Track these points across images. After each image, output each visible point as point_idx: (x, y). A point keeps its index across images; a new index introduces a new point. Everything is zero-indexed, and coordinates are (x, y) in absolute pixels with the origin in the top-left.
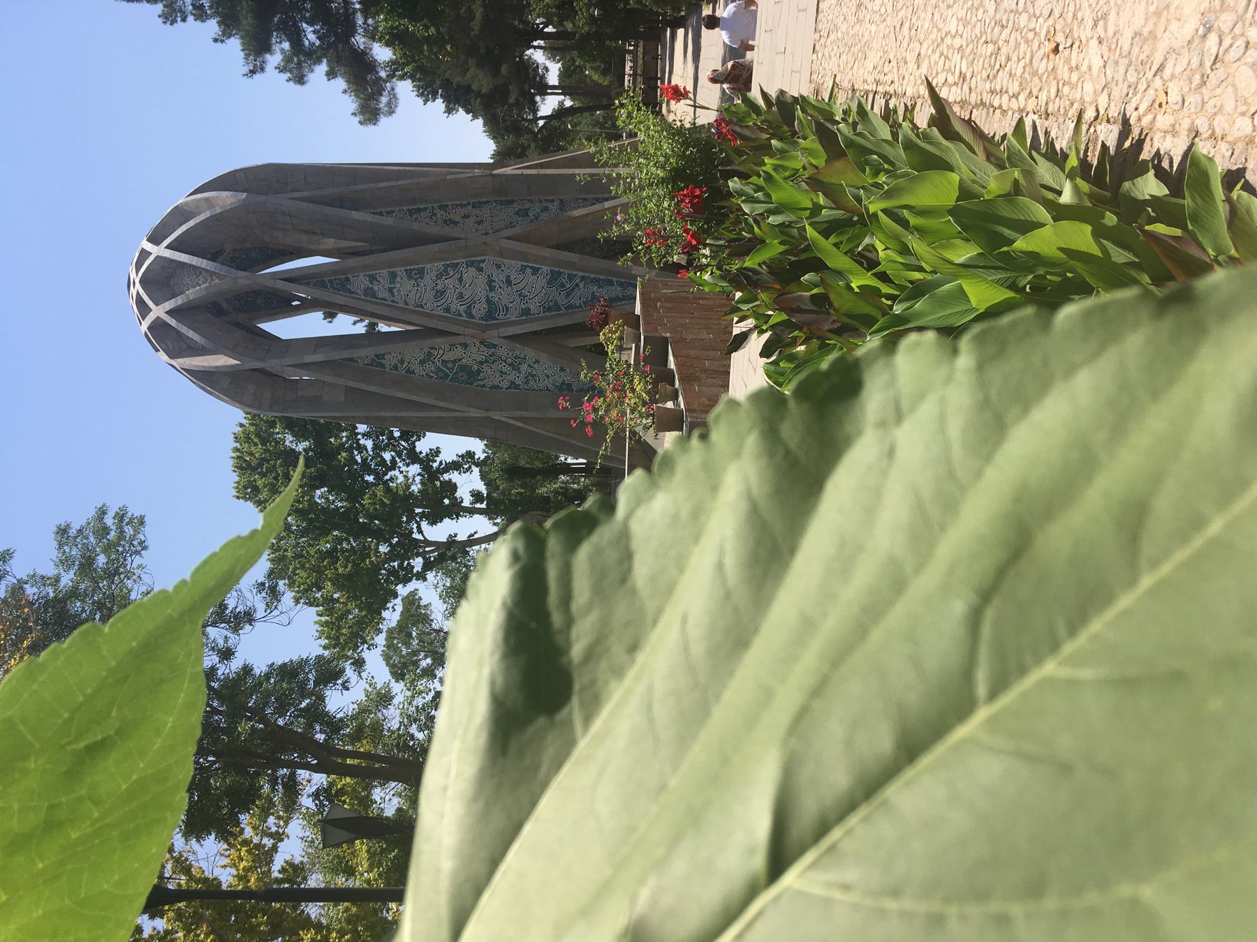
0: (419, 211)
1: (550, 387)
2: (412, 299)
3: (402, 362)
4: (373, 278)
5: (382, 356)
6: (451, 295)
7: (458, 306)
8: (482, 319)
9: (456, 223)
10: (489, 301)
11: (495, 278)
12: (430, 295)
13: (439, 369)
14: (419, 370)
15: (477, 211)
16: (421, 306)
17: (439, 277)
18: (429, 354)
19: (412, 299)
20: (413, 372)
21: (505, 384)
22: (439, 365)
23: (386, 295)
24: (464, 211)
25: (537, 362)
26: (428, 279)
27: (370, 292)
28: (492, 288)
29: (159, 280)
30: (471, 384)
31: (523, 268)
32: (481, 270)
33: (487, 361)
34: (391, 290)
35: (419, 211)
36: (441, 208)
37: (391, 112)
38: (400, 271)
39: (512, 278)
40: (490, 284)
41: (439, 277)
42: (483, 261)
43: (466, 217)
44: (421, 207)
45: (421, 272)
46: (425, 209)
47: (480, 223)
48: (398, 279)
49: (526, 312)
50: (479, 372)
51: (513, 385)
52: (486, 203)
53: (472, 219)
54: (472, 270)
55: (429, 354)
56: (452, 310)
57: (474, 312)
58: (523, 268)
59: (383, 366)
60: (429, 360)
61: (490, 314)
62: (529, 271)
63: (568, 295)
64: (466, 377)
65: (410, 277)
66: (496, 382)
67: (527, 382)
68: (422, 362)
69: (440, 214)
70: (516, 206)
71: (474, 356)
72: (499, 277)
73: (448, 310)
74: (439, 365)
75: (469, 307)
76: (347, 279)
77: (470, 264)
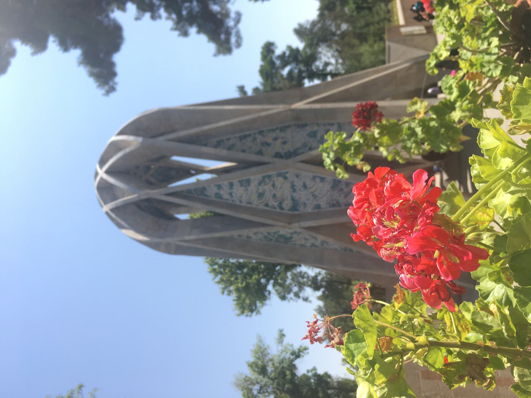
0: (246, 137)
2: (244, 199)
6: (268, 196)
7: (273, 203)
8: (289, 210)
9: (268, 144)
10: (293, 199)
11: (296, 183)
12: (254, 197)
15: (282, 134)
16: (250, 203)
17: (260, 184)
19: (244, 199)
20: (251, 238)
21: (308, 244)
24: (274, 135)
26: (253, 186)
27: (218, 196)
28: (294, 191)
29: (105, 191)
31: (314, 178)
32: (286, 178)
34: (231, 194)
35: (246, 137)
36: (261, 133)
37: (239, 45)
38: (235, 182)
39: (307, 184)
40: (293, 187)
43: (275, 139)
44: (247, 133)
45: (248, 182)
46: (250, 135)
48: (235, 187)
49: (318, 207)
50: (291, 238)
51: (313, 245)
52: (289, 127)
54: (281, 179)
56: (270, 203)
57: (284, 205)
58: (314, 178)
61: (294, 207)
62: (318, 180)
63: (346, 196)
65: (242, 185)
66: (303, 242)
69: (259, 138)
70: (308, 129)
72: (298, 183)
73: (267, 205)
75: (280, 203)
77: (279, 175)
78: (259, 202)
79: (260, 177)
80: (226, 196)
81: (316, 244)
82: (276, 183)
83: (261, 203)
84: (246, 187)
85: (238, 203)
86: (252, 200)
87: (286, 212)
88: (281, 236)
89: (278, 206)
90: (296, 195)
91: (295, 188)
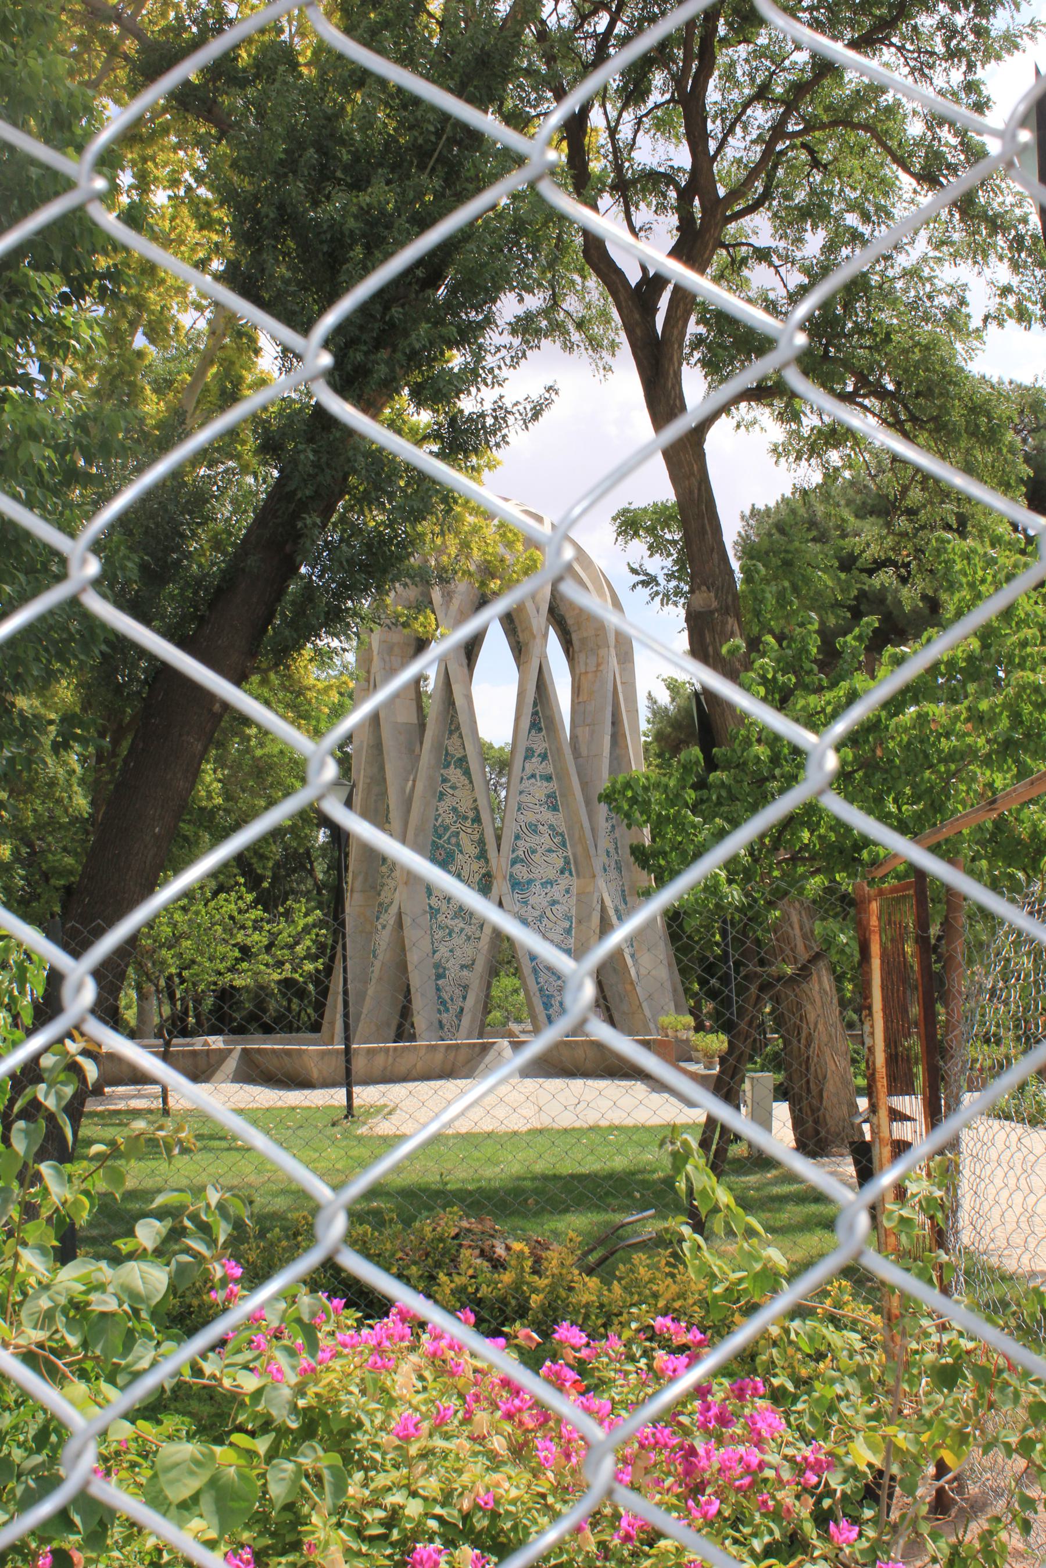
1: (437, 955)
3: (454, 788)
4: (544, 757)
6: (533, 840)
10: (530, 882)
12: (531, 817)
13: (446, 828)
14: (444, 806)
17: (551, 827)
18: (466, 818)
20: (440, 799)
23: (529, 771)
25: (469, 938)
26: (548, 816)
34: (533, 776)
38: (554, 785)
40: (551, 883)
41: (551, 827)
45: (555, 808)
54: (560, 863)
55: (466, 818)
57: (518, 866)
58: (569, 918)
62: (567, 924)
65: (548, 796)
67: (440, 927)
68: (455, 810)
71: (466, 867)
72: (556, 892)
76: (540, 730)
77: (567, 862)
79: (563, 829)
81: (441, 917)
90: (536, 888)
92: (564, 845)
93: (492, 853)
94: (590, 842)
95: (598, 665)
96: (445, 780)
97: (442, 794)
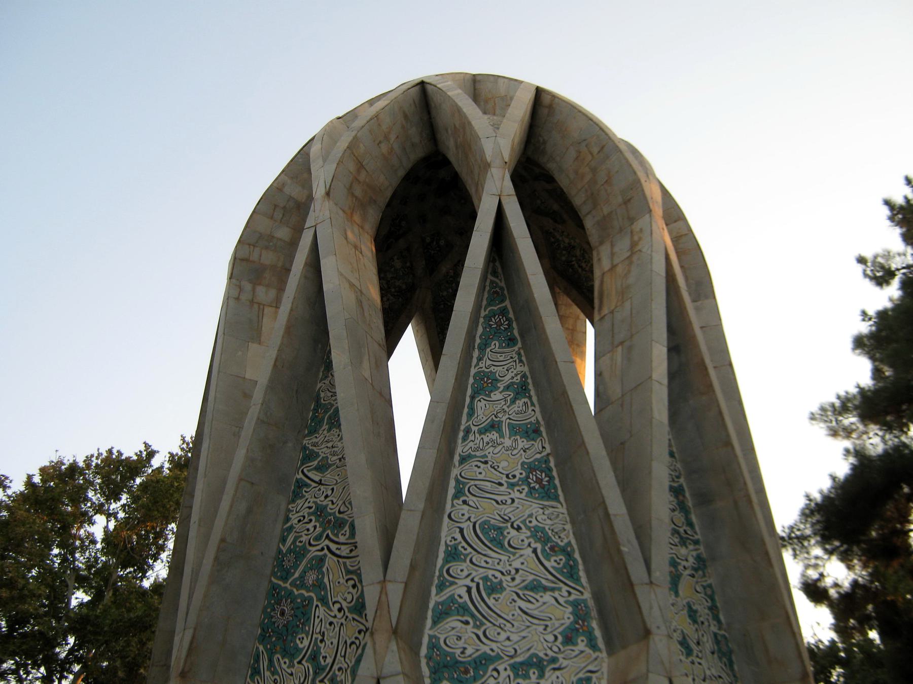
5: (335, 422)
6: (494, 563)
10: (483, 662)
12: (487, 511)
13: (299, 553)
14: (302, 507)
16: (458, 494)
17: (539, 534)
18: (339, 524)
22: (313, 552)
27: (486, 384)
28: (521, 669)
30: (263, 639)
32: (569, 640)
33: (318, 669)
34: (494, 426)
41: (539, 534)
42: (593, 646)
43: (693, 614)
44: (693, 518)
45: (547, 493)
46: (690, 524)
47: (684, 643)
48: (522, 443)
53: (689, 629)
54: (566, 616)
55: (339, 524)
56: (460, 568)
57: (453, 622)
59: (313, 432)
60: (326, 524)
64: (281, 621)
65: (530, 468)
68: (320, 512)
69: (688, 554)
71: (331, 637)
73: (453, 555)
74: (313, 552)
75: (463, 609)
76: (512, 341)
78: (467, 526)
80: (483, 410)
82: (547, 597)
83: (461, 530)
84: (526, 481)
85: (461, 449)
86: (471, 500)
87: (427, 632)
88: (303, 612)
89: (452, 599)
91: (533, 674)
92: (572, 573)
93: (371, 573)
94: (629, 547)
95: (633, 245)
96: (309, 456)
97: (300, 485)
